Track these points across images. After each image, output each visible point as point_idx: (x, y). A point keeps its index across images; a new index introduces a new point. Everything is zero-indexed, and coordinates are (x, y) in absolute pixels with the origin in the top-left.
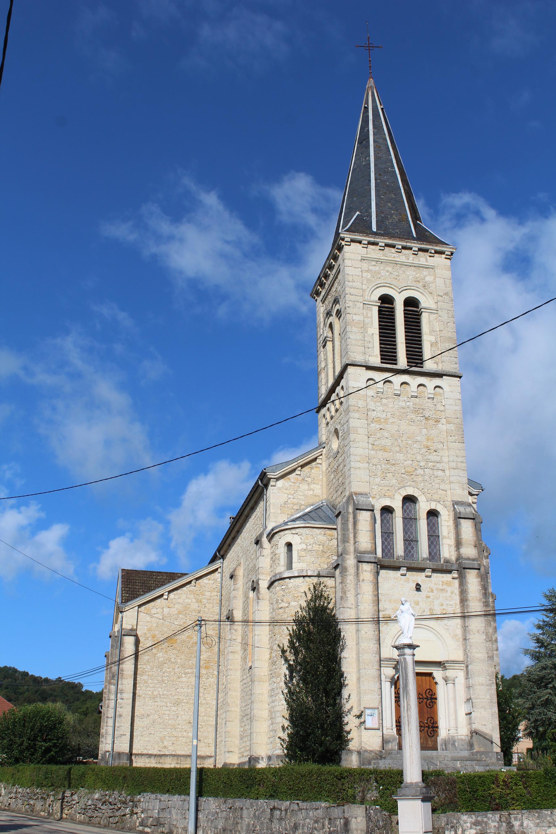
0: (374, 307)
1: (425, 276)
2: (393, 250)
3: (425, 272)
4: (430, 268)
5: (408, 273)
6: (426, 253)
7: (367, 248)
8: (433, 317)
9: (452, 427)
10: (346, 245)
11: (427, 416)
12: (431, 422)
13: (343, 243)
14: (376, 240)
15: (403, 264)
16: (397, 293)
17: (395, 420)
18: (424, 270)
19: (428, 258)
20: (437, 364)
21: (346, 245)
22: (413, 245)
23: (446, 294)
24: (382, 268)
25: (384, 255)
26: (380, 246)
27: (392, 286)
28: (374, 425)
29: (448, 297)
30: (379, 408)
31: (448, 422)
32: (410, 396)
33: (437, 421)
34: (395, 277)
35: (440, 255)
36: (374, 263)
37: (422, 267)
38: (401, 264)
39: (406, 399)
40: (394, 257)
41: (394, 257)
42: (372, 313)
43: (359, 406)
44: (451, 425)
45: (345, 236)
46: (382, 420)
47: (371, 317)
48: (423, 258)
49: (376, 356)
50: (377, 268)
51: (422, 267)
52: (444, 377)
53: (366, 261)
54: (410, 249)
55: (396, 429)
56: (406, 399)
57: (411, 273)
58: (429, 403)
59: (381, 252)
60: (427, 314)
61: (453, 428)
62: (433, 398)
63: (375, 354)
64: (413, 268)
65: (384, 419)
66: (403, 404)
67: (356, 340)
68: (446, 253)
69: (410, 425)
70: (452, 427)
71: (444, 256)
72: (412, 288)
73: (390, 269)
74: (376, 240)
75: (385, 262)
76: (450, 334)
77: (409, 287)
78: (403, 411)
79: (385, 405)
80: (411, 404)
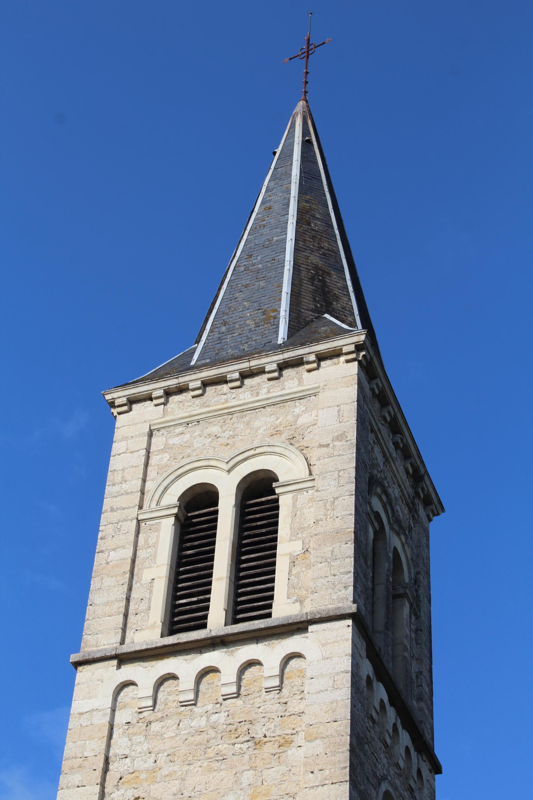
0: (164, 521)
1: (298, 416)
2: (225, 388)
3: (299, 408)
4: (310, 396)
5: (257, 424)
6: (301, 368)
7: (164, 404)
8: (303, 497)
9: (318, 747)
10: (119, 413)
11: (260, 735)
12: (269, 748)
13: (115, 411)
14: (181, 380)
15: (245, 410)
16: (225, 474)
17: (176, 768)
18: (297, 403)
19: (306, 375)
20: (301, 602)
21: (119, 413)
22: (264, 361)
23: (340, 437)
24: (196, 434)
25: (204, 405)
26: (194, 390)
27: (212, 463)
28: (122, 791)
29: (343, 443)
30: (139, 749)
31: (310, 739)
32: (220, 699)
33: (286, 742)
34: (225, 441)
35: (335, 360)
36: (180, 429)
37: (292, 400)
38: (242, 411)
39: (210, 707)
40: (226, 401)
41: (226, 401)
42: (158, 537)
43: (86, 754)
44: (318, 742)
45: (115, 395)
46: (143, 776)
47: (155, 545)
48: (292, 382)
49: (153, 626)
50: (187, 437)
51: (292, 400)
52: (311, 628)
53: (162, 431)
54: (261, 371)
55: (174, 790)
56: (210, 707)
57: (263, 421)
58: (270, 704)
59: (197, 401)
60: (290, 495)
61: (320, 750)
62: (280, 688)
63: (151, 622)
64: (268, 409)
65: (147, 771)
66: (203, 722)
67: (107, 604)
68: (345, 350)
69: (211, 770)
70: (318, 747)
71: (342, 359)
72: (258, 451)
73: (215, 429)
74: (181, 380)
75: (204, 419)
76: (338, 523)
77: (252, 452)
78: (198, 738)
79: (160, 735)
80: (221, 718)
